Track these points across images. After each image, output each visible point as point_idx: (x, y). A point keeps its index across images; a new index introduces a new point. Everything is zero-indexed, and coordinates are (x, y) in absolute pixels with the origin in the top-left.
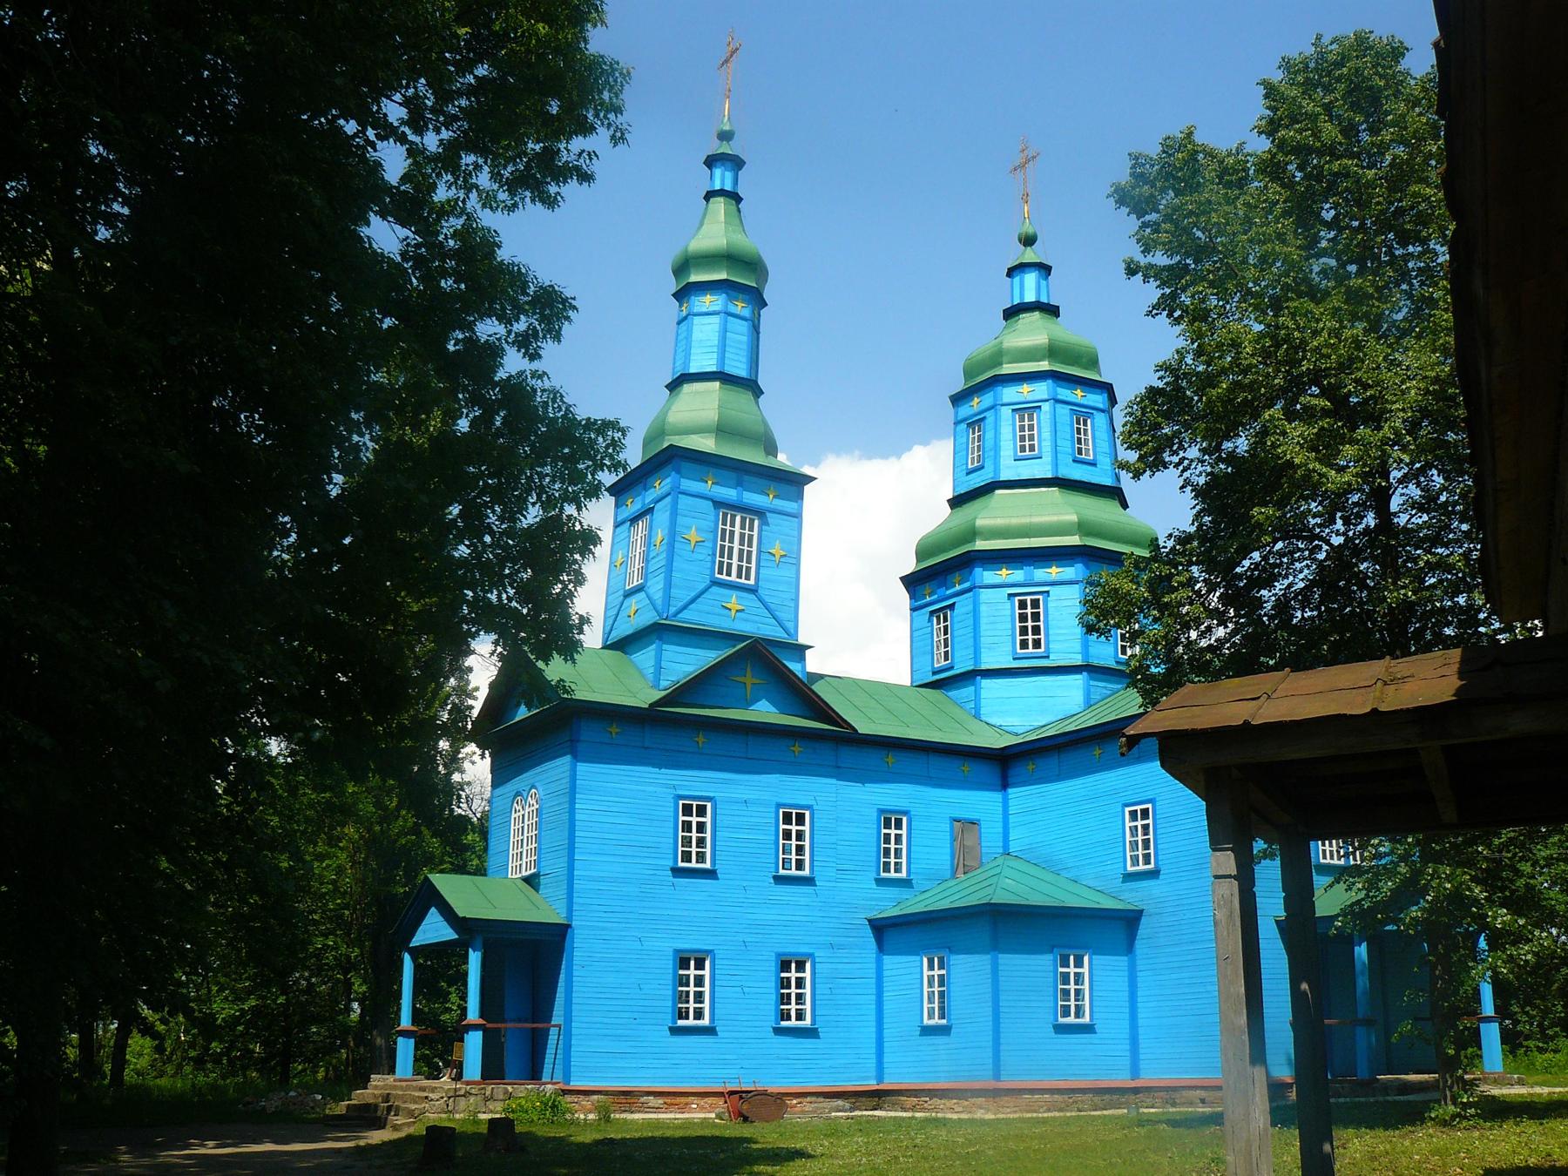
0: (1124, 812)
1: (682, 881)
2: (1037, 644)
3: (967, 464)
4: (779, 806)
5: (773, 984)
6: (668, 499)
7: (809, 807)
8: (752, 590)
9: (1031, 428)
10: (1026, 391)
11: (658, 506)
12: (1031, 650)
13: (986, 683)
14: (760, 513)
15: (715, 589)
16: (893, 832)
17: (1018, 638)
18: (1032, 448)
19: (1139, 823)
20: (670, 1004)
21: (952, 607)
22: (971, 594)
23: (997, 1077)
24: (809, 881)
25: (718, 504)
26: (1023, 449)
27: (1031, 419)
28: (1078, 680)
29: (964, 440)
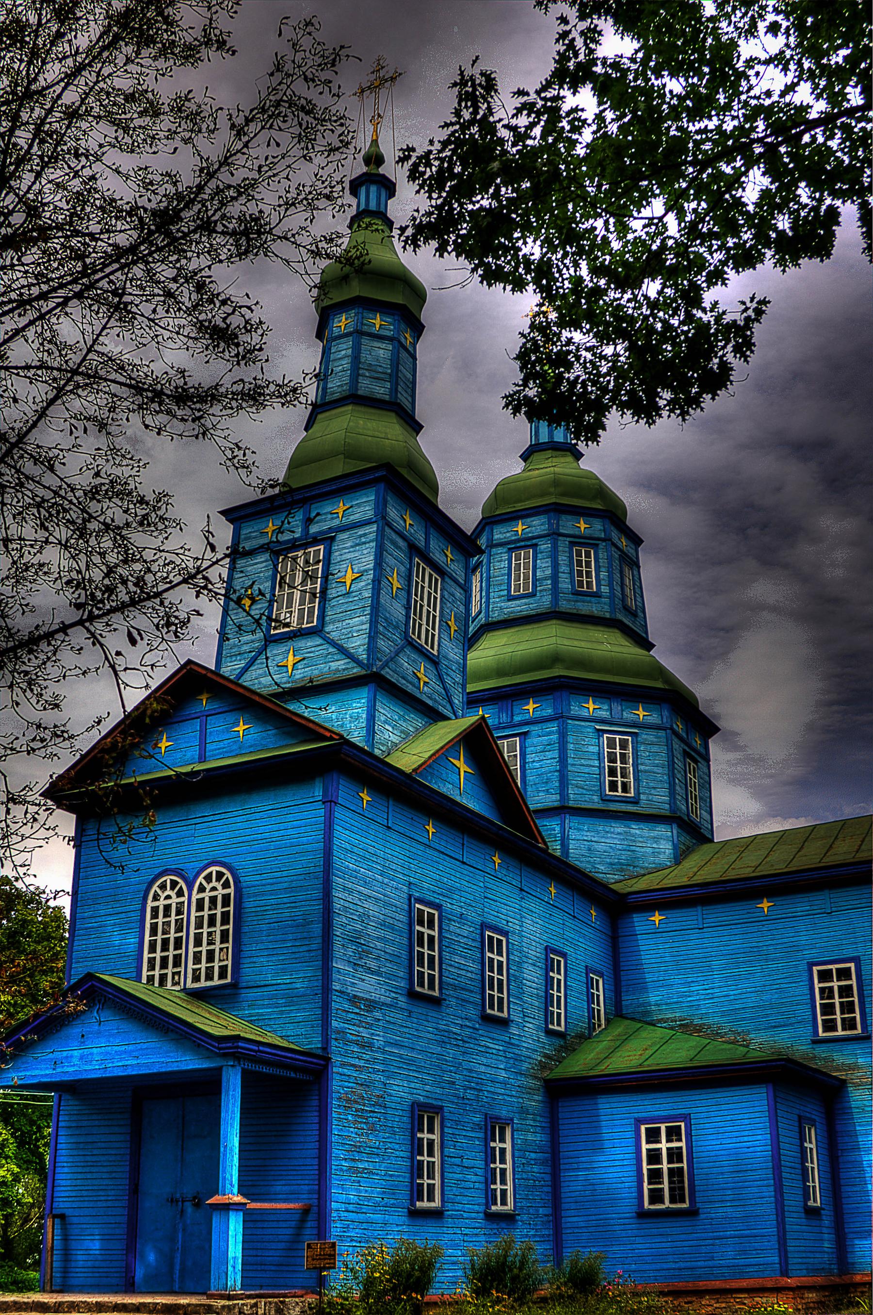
1: (419, 1009)
3: (509, 590)
4: (484, 926)
6: (374, 527)
7: (505, 934)
12: (620, 793)
13: (572, 822)
15: (408, 651)
16: (556, 976)
19: (835, 984)
21: (525, 734)
24: (504, 1023)
28: (664, 831)
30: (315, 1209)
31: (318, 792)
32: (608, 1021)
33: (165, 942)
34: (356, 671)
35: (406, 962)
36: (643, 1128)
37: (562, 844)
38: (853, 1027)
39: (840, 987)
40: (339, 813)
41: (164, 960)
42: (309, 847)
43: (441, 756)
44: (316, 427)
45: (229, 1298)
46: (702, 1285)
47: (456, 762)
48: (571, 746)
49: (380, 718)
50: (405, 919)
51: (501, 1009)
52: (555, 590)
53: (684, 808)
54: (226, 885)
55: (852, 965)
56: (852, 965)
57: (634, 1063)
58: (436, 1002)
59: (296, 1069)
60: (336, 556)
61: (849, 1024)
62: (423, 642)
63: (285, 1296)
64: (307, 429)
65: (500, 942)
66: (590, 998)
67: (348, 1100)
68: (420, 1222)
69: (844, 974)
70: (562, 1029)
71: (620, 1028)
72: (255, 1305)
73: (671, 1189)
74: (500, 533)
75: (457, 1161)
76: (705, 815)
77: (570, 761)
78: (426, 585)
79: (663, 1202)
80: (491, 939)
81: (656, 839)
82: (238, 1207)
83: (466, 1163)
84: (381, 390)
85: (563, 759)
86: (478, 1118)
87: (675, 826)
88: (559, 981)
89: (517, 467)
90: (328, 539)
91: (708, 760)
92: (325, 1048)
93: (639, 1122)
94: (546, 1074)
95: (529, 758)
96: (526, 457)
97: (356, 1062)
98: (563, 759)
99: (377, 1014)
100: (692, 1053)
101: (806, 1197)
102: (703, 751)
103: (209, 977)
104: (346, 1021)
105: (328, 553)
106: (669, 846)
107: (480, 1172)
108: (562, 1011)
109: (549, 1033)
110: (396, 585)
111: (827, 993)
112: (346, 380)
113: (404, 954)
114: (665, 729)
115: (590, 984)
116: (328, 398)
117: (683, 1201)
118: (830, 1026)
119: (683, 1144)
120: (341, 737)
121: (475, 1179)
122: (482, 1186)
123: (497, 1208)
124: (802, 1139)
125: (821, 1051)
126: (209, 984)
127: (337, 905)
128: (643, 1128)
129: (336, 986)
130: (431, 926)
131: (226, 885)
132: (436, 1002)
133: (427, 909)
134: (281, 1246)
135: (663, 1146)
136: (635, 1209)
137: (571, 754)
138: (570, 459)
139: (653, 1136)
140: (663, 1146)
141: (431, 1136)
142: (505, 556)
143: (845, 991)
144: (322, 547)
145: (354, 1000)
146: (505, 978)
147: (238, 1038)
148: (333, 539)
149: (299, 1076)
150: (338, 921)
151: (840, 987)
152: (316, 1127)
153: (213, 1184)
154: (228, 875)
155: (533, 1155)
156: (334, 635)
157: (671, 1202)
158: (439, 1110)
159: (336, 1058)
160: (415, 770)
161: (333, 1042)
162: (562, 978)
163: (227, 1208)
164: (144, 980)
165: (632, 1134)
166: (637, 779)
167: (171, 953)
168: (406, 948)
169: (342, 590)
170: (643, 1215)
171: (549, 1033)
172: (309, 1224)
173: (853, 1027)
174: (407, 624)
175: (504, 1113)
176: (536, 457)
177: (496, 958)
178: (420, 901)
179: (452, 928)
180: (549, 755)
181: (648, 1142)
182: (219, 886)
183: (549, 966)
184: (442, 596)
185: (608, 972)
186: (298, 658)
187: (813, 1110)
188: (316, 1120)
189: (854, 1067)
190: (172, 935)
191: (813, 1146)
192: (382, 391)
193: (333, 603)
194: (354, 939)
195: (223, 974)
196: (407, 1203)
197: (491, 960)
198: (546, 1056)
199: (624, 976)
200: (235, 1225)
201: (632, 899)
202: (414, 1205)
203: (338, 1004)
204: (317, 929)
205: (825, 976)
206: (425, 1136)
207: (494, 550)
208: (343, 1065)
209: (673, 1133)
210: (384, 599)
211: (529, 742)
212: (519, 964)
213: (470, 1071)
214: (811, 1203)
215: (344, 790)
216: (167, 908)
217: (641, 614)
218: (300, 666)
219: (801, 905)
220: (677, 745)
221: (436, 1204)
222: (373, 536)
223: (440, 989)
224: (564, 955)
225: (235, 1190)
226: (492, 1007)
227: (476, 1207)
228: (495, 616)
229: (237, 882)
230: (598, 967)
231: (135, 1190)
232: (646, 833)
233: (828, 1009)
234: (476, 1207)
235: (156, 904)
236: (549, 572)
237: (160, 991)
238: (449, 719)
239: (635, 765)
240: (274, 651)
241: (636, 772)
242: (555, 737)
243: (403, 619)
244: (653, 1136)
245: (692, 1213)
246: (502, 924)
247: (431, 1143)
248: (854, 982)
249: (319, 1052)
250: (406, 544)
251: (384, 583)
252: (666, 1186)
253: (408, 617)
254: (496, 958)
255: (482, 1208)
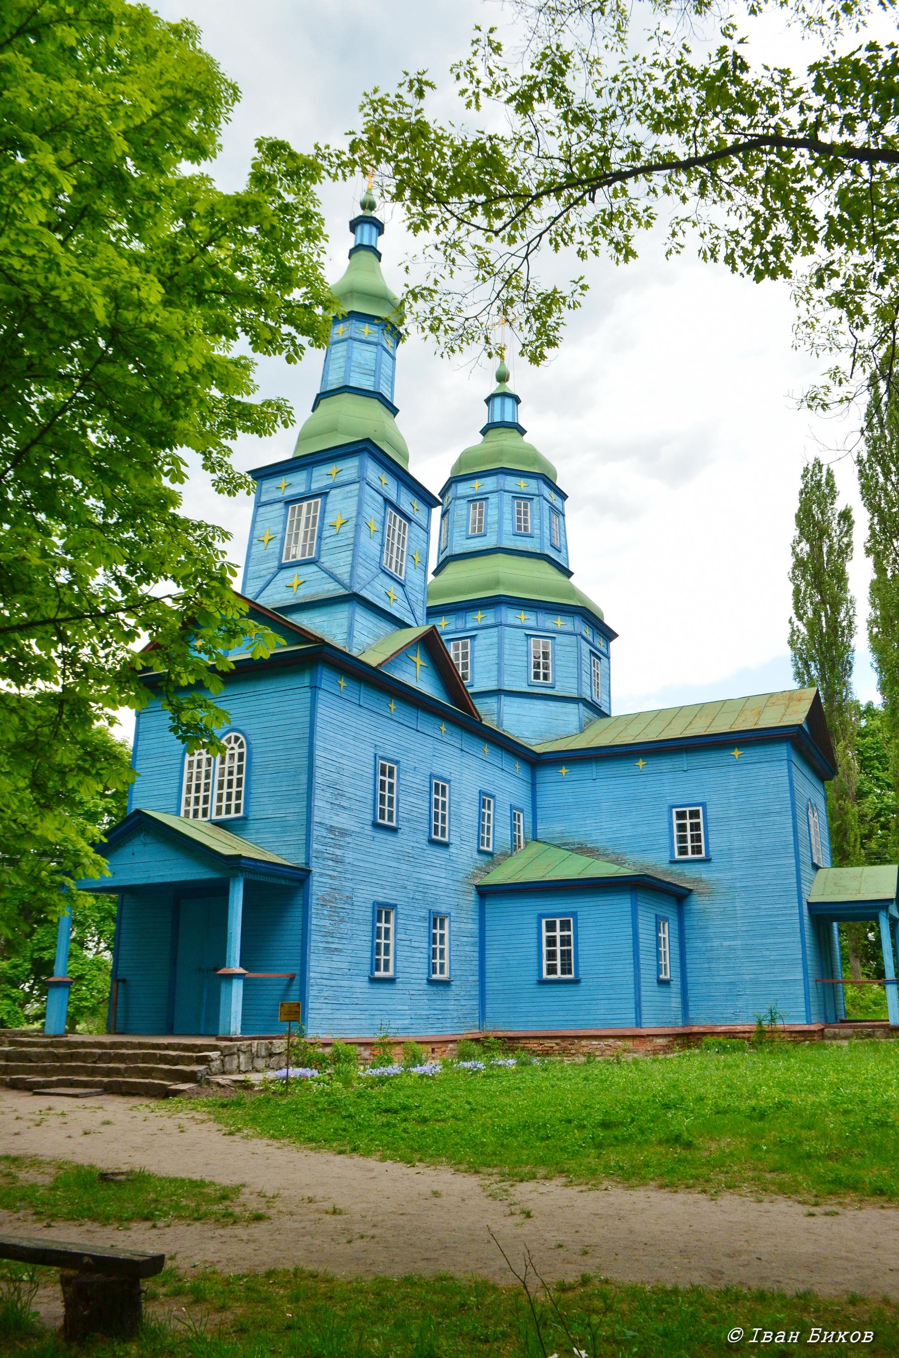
0: (671, 812)
1: (381, 836)
2: (546, 677)
3: (467, 531)
4: (432, 776)
5: (427, 939)
6: (357, 486)
7: (449, 781)
8: (403, 586)
9: (526, 514)
10: (522, 485)
11: (333, 492)
12: (541, 680)
13: (505, 700)
14: (409, 520)
15: (382, 576)
16: (486, 811)
17: (533, 670)
18: (526, 528)
19: (688, 822)
20: (368, 954)
21: (473, 637)
22: (495, 629)
23: (639, 1024)
24: (446, 845)
25: (387, 501)
26: (519, 528)
27: (526, 506)
28: (572, 708)
29: (464, 512)
30: (297, 978)
31: (306, 680)
32: (526, 843)
33: (198, 787)
34: (343, 592)
35: (371, 802)
36: (544, 922)
37: (499, 717)
38: (700, 852)
39: (691, 824)
40: (321, 695)
41: (197, 799)
42: (300, 720)
43: (401, 654)
44: (319, 409)
45: (231, 1040)
46: (581, 1033)
47: (414, 658)
48: (507, 646)
49: (357, 626)
50: (372, 772)
51: (443, 835)
52: (500, 531)
53: (589, 692)
54: (241, 746)
55: (700, 809)
56: (700, 809)
57: (541, 874)
58: (394, 830)
59: (285, 878)
60: (329, 507)
61: (697, 850)
62: (393, 570)
63: (274, 1038)
64: (313, 410)
65: (444, 787)
66: (514, 828)
67: (324, 900)
68: (377, 986)
69: (694, 814)
70: (490, 849)
71: (536, 847)
72: (250, 1045)
73: (562, 965)
74: (463, 489)
75: (407, 943)
76: (606, 698)
77: (506, 657)
78: (397, 528)
79: (555, 973)
80: (437, 785)
81: (566, 714)
82: (239, 976)
83: (414, 944)
84: (367, 384)
85: (500, 656)
86: (424, 913)
87: (581, 705)
88: (489, 815)
89: (478, 439)
90: (323, 494)
91: (609, 658)
92: (307, 864)
93: (541, 916)
94: (478, 882)
95: (476, 654)
96: (484, 432)
97: (331, 873)
98: (500, 656)
99: (348, 839)
100: (580, 869)
101: (659, 971)
102: (605, 651)
103: (228, 811)
104: (325, 845)
105: (324, 504)
106: (576, 718)
107: (424, 951)
108: (491, 836)
109: (480, 852)
110: (373, 528)
111: (682, 827)
112: (342, 375)
113: (371, 797)
114: (576, 635)
115: (514, 817)
116: (329, 388)
117: (570, 973)
118: (683, 851)
119: (571, 933)
120: (322, 641)
121: (422, 956)
122: (426, 961)
123: (437, 976)
124: (658, 930)
125: (676, 868)
126: (228, 816)
127: (318, 762)
128: (544, 922)
129: (316, 819)
130: (391, 775)
131: (241, 746)
132: (394, 830)
133: (388, 764)
134: (275, 1002)
135: (558, 934)
136: (536, 978)
137: (507, 651)
138: (516, 434)
139: (551, 927)
140: (558, 934)
141: (387, 926)
142: (465, 506)
143: (695, 827)
144: (319, 500)
145: (331, 829)
146: (447, 813)
147: (240, 856)
148: (327, 493)
149: (288, 883)
150: (318, 773)
151: (691, 824)
152: (300, 919)
153: (222, 960)
154: (242, 739)
155: (465, 939)
156: (326, 565)
157: (563, 973)
158: (394, 907)
159: (315, 869)
160: (380, 665)
161: (314, 859)
162: (491, 813)
163: (231, 977)
164: (182, 814)
165: (535, 925)
166: (554, 671)
167: (202, 794)
168: (372, 792)
169: (334, 532)
170: (542, 982)
171: (480, 852)
172: (294, 988)
173: (700, 852)
174: (381, 558)
175: (443, 909)
176: (491, 433)
177: (440, 798)
178: (382, 758)
179: (407, 778)
180: (491, 652)
181: (548, 931)
182: (236, 746)
183: (483, 804)
184: (409, 537)
185: (528, 809)
186: (302, 580)
187: (668, 911)
188: (300, 914)
189: (700, 881)
190: (203, 781)
191: (666, 936)
192: (368, 383)
193: (327, 541)
194: (332, 786)
195: (237, 810)
196: (368, 973)
197: (437, 800)
198: (477, 868)
199: (539, 812)
200: (237, 988)
201: (544, 757)
202: (372, 973)
203: (317, 831)
204: (304, 778)
205: (681, 815)
206: (383, 925)
207: (458, 502)
208: (321, 875)
209: (565, 925)
210: (364, 537)
211: (476, 643)
212: (458, 804)
213: (419, 879)
214: (662, 976)
215: (327, 679)
216: (199, 761)
217: (563, 550)
218: (301, 587)
219: (666, 764)
220: (586, 647)
221: (390, 974)
222: (356, 492)
223: (397, 821)
224: (493, 797)
225: (238, 964)
226: (436, 833)
227: (421, 976)
228: (457, 550)
229: (248, 744)
230: (521, 806)
231: (174, 963)
232: (560, 710)
233: (682, 839)
234: (421, 976)
235: (192, 758)
236: (496, 518)
237: (186, 820)
238: (409, 626)
239: (553, 661)
240: (284, 574)
241: (554, 665)
242: (495, 640)
243: (379, 554)
244: (551, 927)
245: (576, 982)
246: (446, 775)
247: (387, 930)
248: (701, 820)
249: (304, 866)
250: (380, 499)
251: (364, 528)
252: (558, 962)
253: (382, 552)
254: (440, 798)
255: (426, 976)
